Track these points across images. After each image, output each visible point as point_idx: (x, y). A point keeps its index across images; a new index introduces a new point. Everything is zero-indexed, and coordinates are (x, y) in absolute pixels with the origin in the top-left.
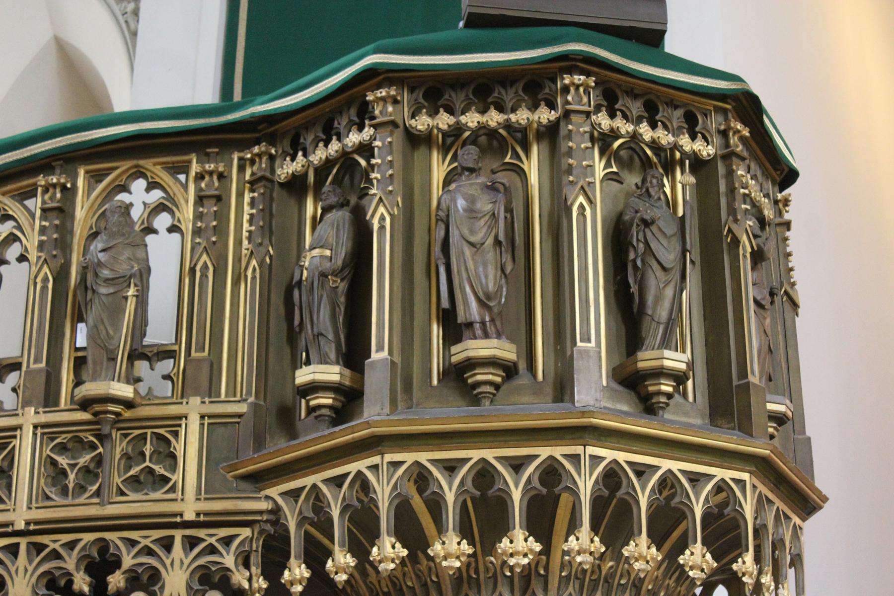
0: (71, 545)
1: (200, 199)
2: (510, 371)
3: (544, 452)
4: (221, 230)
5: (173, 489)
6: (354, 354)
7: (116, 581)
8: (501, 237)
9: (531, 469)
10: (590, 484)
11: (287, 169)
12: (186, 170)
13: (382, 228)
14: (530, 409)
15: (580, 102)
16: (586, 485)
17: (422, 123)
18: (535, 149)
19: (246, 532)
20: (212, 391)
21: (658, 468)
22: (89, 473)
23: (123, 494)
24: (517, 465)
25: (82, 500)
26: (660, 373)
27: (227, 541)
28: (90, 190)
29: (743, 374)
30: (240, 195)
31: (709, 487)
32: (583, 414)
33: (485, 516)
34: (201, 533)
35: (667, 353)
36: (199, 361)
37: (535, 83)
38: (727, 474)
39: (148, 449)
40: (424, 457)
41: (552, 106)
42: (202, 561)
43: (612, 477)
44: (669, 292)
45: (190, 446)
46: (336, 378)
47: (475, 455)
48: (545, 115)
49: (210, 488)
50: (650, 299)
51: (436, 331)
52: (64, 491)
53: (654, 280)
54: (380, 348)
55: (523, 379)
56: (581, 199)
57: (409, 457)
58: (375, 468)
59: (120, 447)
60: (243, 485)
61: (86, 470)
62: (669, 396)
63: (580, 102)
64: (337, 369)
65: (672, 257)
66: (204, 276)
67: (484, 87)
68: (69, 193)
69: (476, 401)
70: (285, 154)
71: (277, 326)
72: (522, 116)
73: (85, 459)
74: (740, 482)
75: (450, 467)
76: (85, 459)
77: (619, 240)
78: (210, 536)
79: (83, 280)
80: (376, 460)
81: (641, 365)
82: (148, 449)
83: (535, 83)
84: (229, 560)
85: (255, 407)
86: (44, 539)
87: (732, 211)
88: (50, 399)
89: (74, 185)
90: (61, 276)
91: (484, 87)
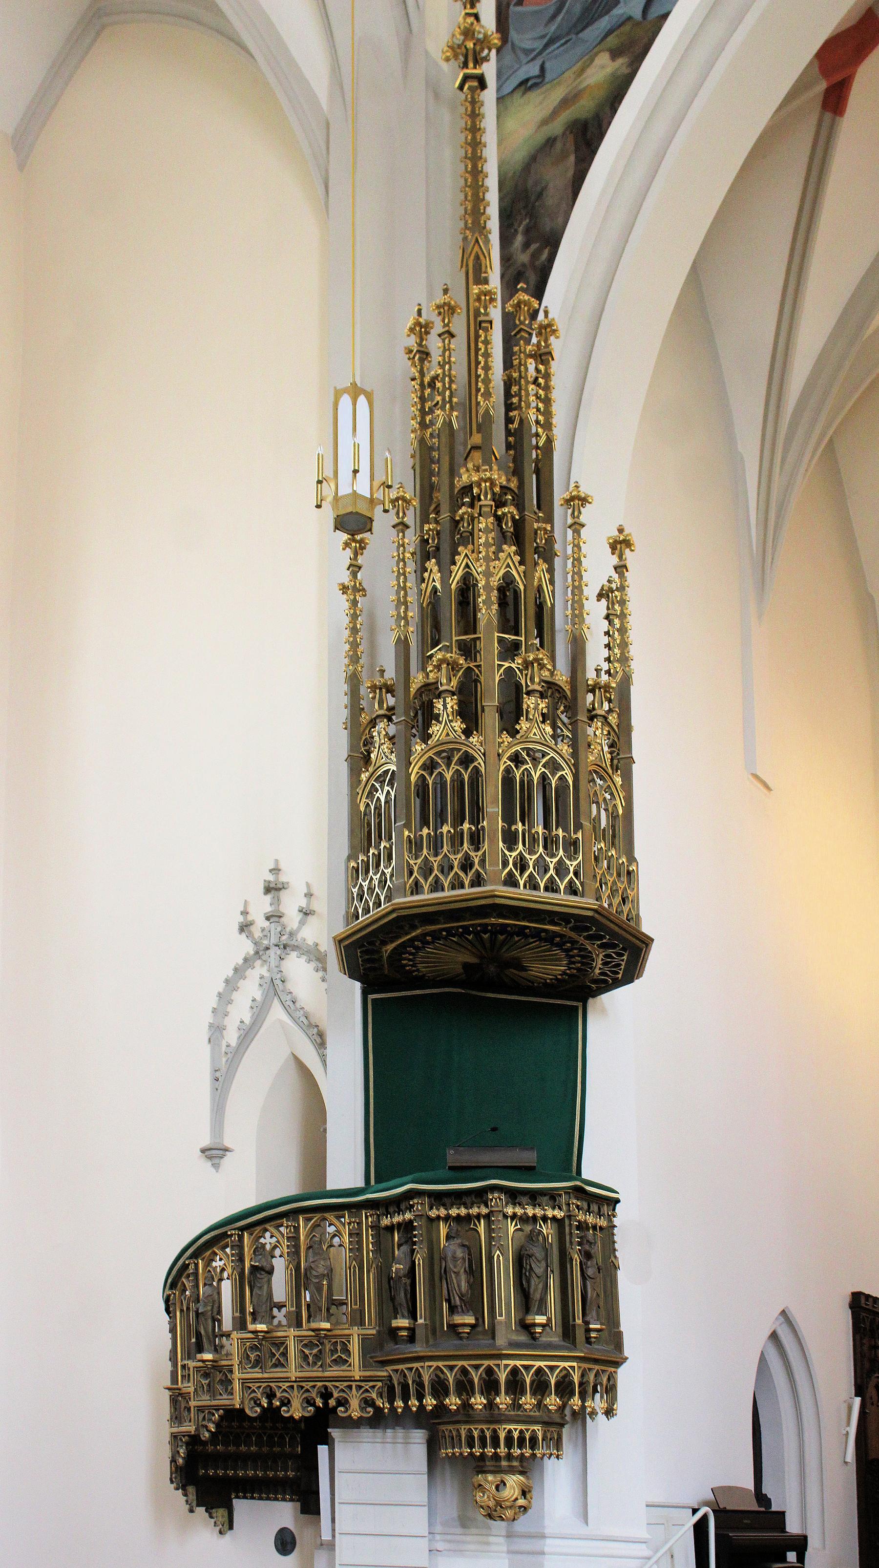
0: (314, 1387)
1: (350, 1235)
2: (473, 1327)
3: (486, 1363)
4: (360, 1249)
5: (350, 1365)
6: (413, 1316)
7: (332, 1402)
8: (467, 1269)
9: (481, 1369)
10: (504, 1376)
11: (386, 1221)
12: (344, 1217)
13: (419, 1264)
14: (482, 1345)
15: (498, 1206)
16: (503, 1377)
17: (433, 1213)
18: (482, 1221)
19: (380, 1384)
20: (362, 1323)
21: (534, 1366)
22: (318, 1357)
23: (331, 1366)
24: (477, 1367)
25: (315, 1369)
26: (535, 1325)
27: (373, 1387)
28: (306, 1225)
29: (574, 1320)
30: (367, 1230)
31: (558, 1371)
32: (499, 1350)
33: (465, 1387)
34: (362, 1384)
35: (537, 1317)
36: (356, 1310)
37: (480, 1195)
38: (566, 1364)
39: (339, 1348)
40: (440, 1364)
41: (487, 1206)
42: (363, 1396)
43: (515, 1371)
44: (541, 1286)
45: (355, 1347)
46: (407, 1325)
47: (460, 1363)
48: (484, 1211)
49: (365, 1366)
50: (532, 1291)
51: (445, 1305)
52: (308, 1364)
53: (534, 1281)
54: (421, 1318)
55: (480, 1329)
56: (498, 1252)
57: (434, 1364)
58: (422, 1367)
59: (328, 1347)
60: (377, 1364)
61: (316, 1355)
62: (540, 1333)
63: (498, 1206)
64: (407, 1321)
65: (542, 1270)
66: (355, 1271)
67: (458, 1197)
68: (297, 1229)
69: (461, 1339)
70: (384, 1214)
71: (385, 1295)
72: (474, 1211)
73: (315, 1351)
74: (573, 1368)
75: (451, 1368)
76: (315, 1351)
77: (521, 1261)
78: (367, 1385)
79: (306, 1274)
80: (422, 1364)
81: (527, 1322)
82: (339, 1348)
83: (480, 1195)
84: (374, 1396)
85: (378, 1332)
86: (303, 1384)
87: (571, 1243)
88: (299, 1325)
89: (299, 1225)
90: (298, 1268)
91: (458, 1197)
